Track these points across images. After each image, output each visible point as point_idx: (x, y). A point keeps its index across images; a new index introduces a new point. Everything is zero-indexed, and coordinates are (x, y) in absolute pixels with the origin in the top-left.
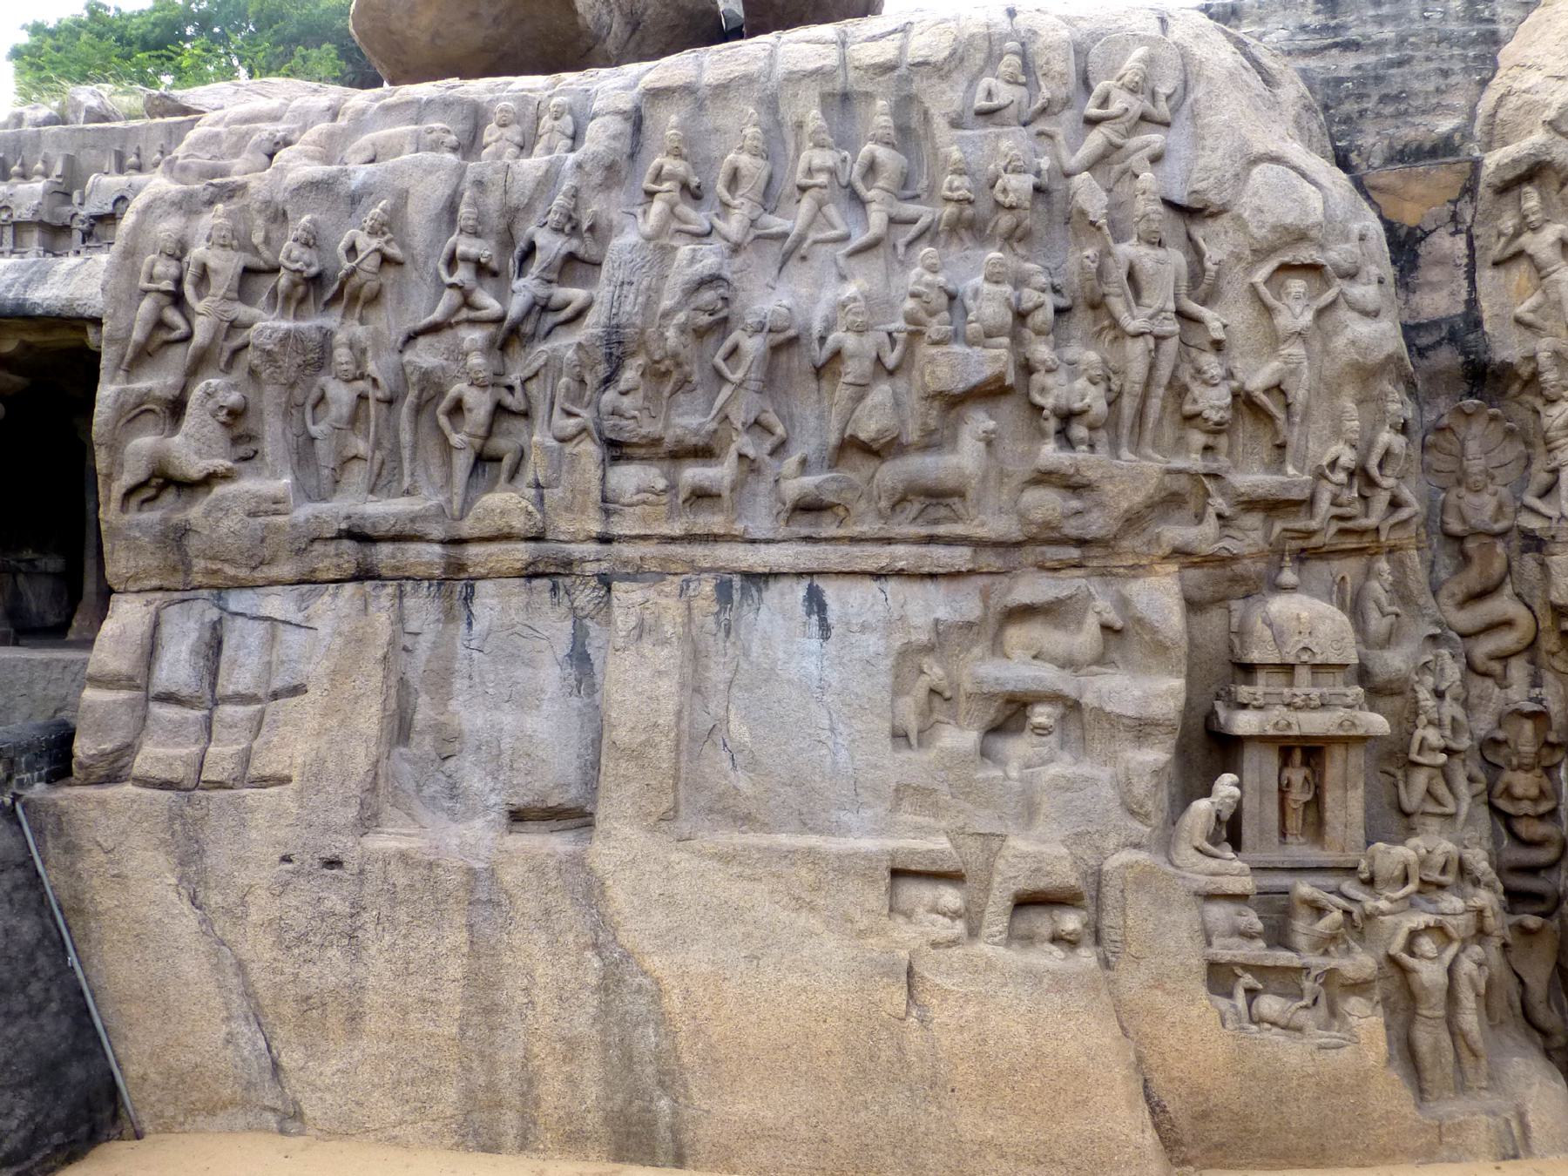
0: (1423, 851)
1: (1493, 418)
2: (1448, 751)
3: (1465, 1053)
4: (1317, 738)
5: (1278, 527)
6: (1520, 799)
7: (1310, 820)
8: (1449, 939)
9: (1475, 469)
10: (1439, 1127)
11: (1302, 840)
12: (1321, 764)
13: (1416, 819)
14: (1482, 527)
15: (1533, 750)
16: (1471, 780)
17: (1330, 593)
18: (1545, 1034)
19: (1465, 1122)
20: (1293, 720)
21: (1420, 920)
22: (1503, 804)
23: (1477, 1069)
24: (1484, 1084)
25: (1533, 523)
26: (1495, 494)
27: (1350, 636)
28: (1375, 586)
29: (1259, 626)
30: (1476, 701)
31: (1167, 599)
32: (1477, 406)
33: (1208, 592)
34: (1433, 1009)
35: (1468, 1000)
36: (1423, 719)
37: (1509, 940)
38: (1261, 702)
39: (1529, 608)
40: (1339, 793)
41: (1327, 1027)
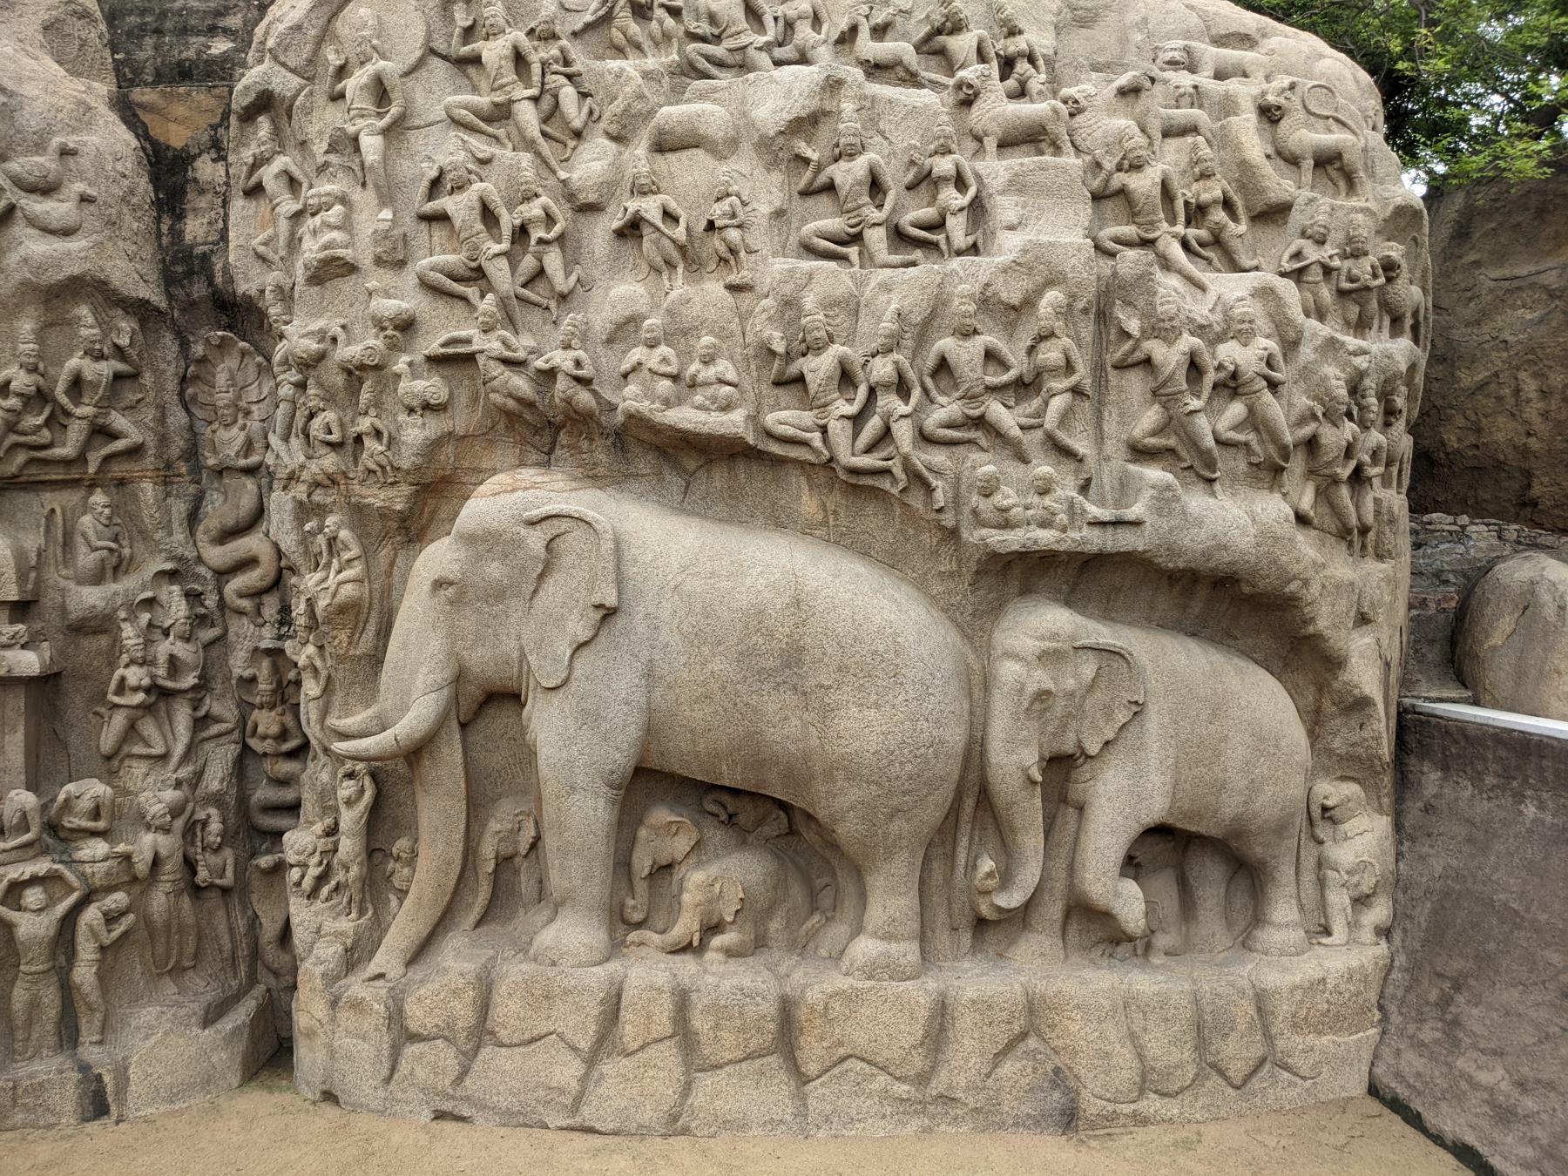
1: (243, 353)
2: (160, 695)
3: (81, 1008)
6: (264, 738)
9: (220, 403)
10: (14, 1088)
13: (116, 763)
18: (276, 974)
19: (49, 1081)
21: (42, 866)
22: (253, 743)
25: (270, 460)
26: (243, 428)
27: (11, 573)
28: (87, 520)
32: (223, 338)
34: (33, 965)
35: (87, 951)
36: (125, 658)
37: (229, 879)
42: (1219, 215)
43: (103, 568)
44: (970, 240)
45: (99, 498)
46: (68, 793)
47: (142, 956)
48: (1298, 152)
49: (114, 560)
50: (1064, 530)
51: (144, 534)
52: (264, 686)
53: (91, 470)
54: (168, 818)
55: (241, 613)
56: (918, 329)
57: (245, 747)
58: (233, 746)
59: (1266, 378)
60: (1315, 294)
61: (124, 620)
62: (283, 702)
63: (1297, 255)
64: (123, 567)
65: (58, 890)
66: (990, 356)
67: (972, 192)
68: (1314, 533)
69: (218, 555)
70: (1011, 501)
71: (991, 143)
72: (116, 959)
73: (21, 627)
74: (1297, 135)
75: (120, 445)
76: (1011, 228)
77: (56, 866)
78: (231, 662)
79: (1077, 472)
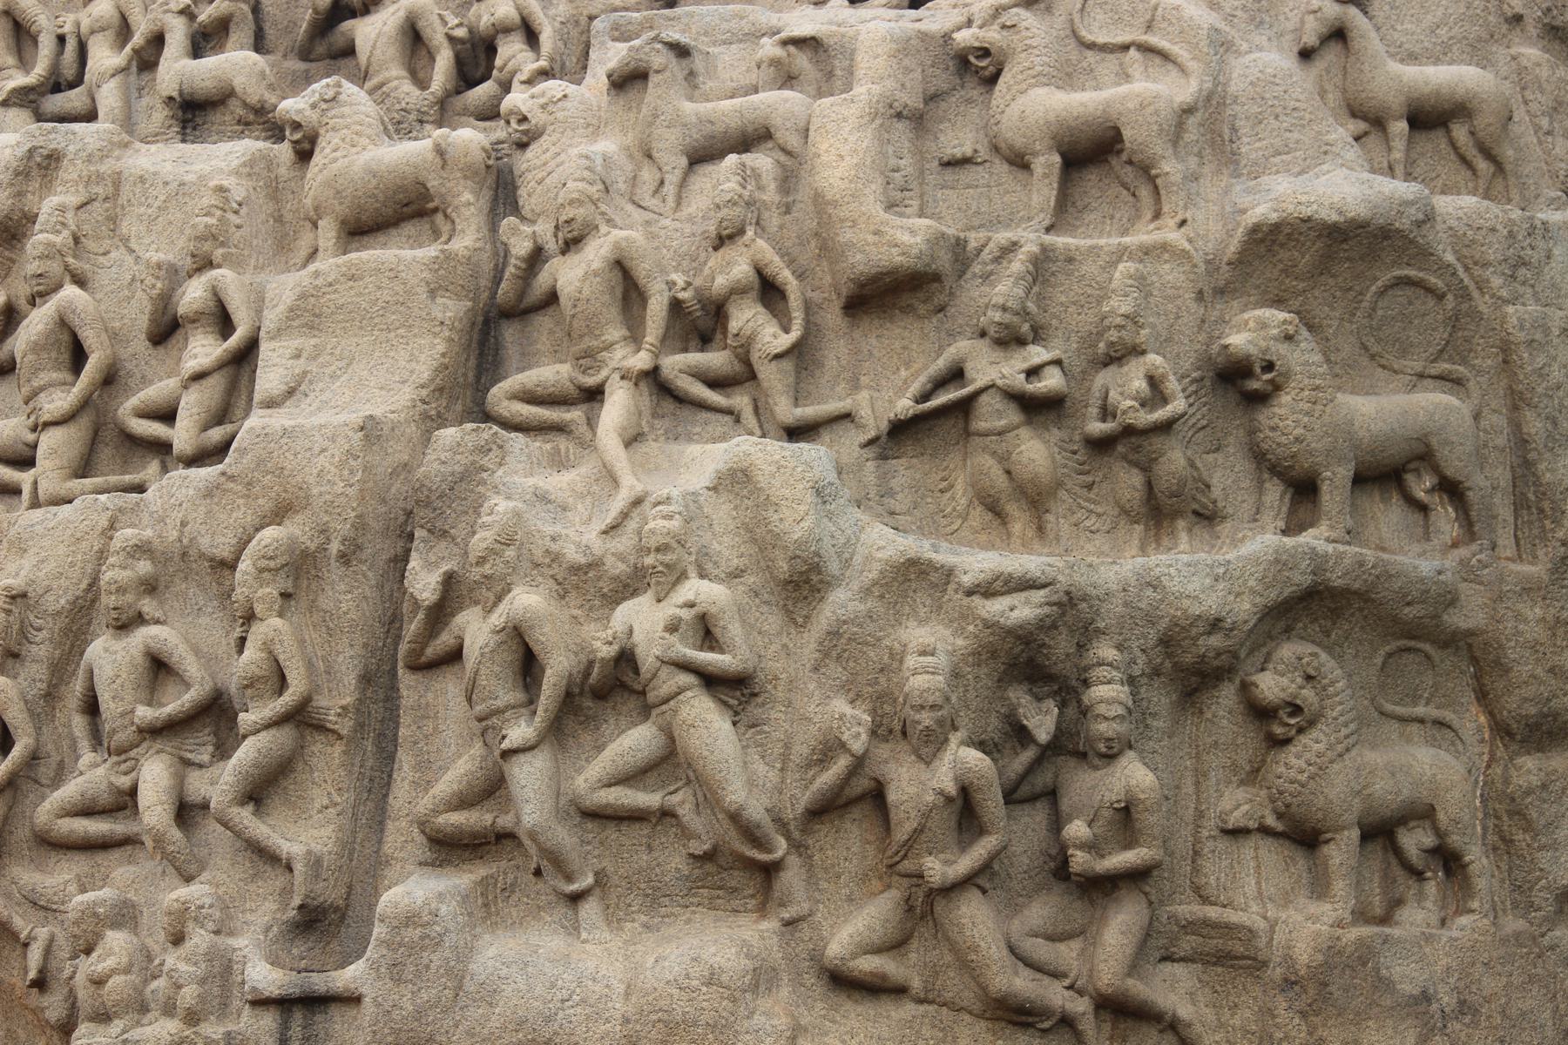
42: (747, 317)
44: (216, 434)
48: (1019, 142)
50: (193, 1018)
56: (62, 622)
59: (685, 666)
60: (1004, 459)
63: (956, 375)
66: (159, 667)
67: (234, 340)
68: (908, 1009)
70: (110, 963)
71: (328, 232)
74: (1016, 108)
76: (271, 404)
79: (287, 892)
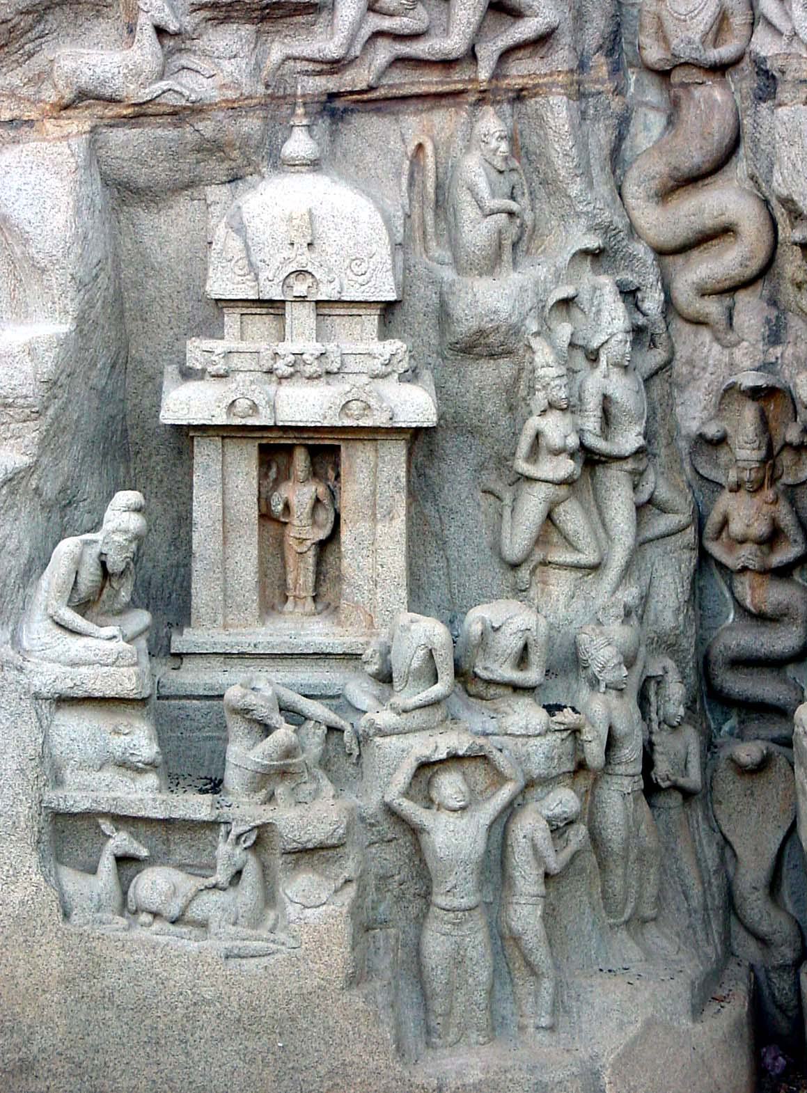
0: (477, 629)
2: (591, 459)
4: (316, 429)
5: (276, 52)
6: (742, 542)
7: (332, 573)
8: (500, 778)
11: (310, 606)
12: (338, 476)
13: (524, 573)
14: (686, 54)
15: (757, 455)
16: (645, 508)
17: (398, 175)
18: (763, 941)
20: (260, 400)
21: (457, 741)
22: (716, 549)
23: (537, 995)
24: (545, 1021)
25: (765, 45)
27: (383, 252)
29: (221, 231)
30: (684, 370)
31: (54, 182)
33: (161, 172)
35: (527, 880)
36: (540, 399)
37: (693, 779)
38: (221, 367)
39: (766, 202)
40: (364, 527)
41: (256, 923)
43: (500, 246)
45: (491, 123)
46: (483, 620)
47: (590, 895)
49: (513, 232)
51: (550, 184)
52: (746, 450)
53: (484, 74)
54: (625, 672)
55: (699, 322)
57: (704, 557)
58: (686, 555)
61: (537, 334)
62: (773, 481)
64: (523, 246)
65: (479, 774)
69: (662, 222)
72: (560, 897)
73: (398, 343)
75: (526, 29)
77: (482, 741)
78: (679, 410)
